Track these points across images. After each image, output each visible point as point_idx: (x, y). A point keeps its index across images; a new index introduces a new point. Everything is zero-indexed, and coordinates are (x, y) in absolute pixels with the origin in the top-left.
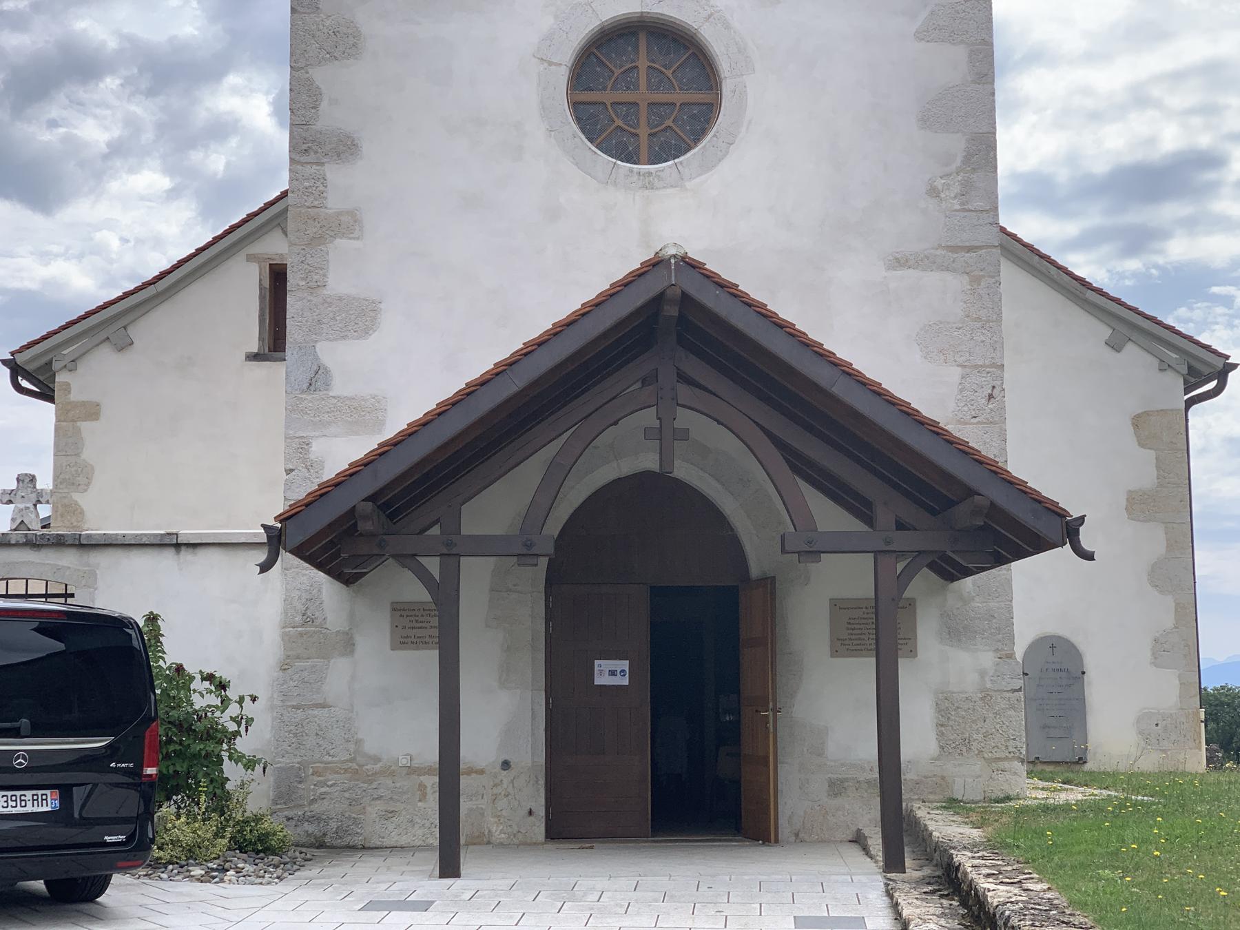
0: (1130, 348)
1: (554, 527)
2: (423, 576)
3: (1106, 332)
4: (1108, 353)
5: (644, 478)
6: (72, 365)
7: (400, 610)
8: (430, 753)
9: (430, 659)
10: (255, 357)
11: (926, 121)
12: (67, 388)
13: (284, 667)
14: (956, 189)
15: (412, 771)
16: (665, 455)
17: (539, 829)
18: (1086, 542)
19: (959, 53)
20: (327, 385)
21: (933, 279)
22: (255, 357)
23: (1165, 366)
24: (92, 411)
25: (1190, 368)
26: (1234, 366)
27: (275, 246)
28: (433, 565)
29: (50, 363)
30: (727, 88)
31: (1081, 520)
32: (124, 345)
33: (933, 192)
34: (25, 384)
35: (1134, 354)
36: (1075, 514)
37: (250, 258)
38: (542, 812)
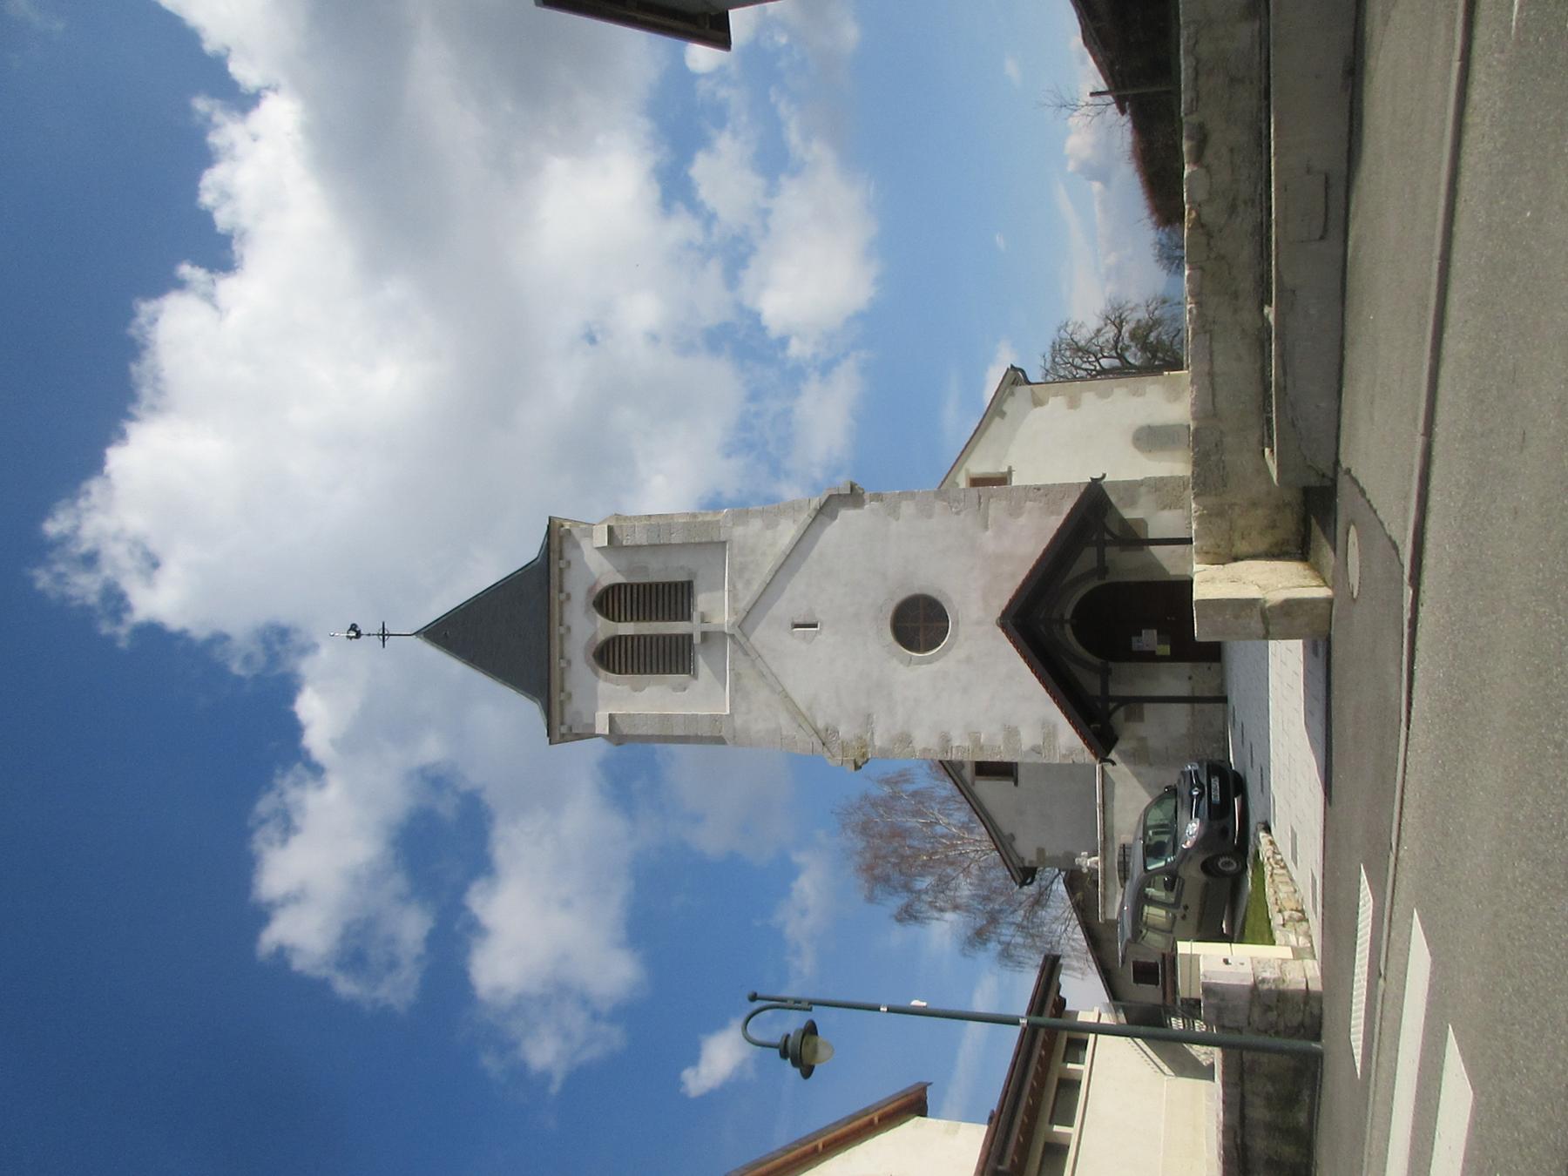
0: (1005, 408)
1: (1096, 661)
2: (1116, 709)
3: (997, 419)
4: (1007, 418)
5: (1073, 627)
6: (1022, 860)
7: (1128, 719)
8: (1185, 708)
9: (1149, 708)
10: (1016, 783)
11: (930, 516)
12: (1031, 862)
13: (1151, 765)
14: (956, 504)
15: (1193, 714)
16: (1067, 621)
17: (1215, 665)
18: (1100, 476)
19: (904, 504)
20: (1039, 746)
21: (991, 512)
22: (1016, 783)
23: (1012, 394)
24: (1041, 851)
25: (1013, 383)
26: (1012, 366)
27: (968, 773)
28: (1112, 706)
29: (1020, 868)
30: (917, 592)
31: (1092, 479)
32: (1012, 837)
33: (958, 513)
34: (1029, 881)
35: (1008, 407)
36: (1090, 480)
37: (973, 784)
38: (1208, 664)
